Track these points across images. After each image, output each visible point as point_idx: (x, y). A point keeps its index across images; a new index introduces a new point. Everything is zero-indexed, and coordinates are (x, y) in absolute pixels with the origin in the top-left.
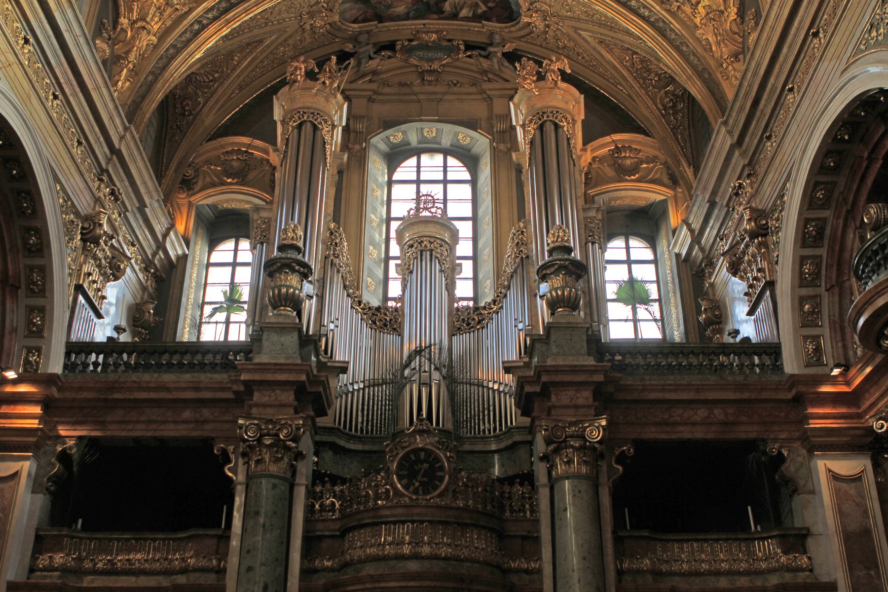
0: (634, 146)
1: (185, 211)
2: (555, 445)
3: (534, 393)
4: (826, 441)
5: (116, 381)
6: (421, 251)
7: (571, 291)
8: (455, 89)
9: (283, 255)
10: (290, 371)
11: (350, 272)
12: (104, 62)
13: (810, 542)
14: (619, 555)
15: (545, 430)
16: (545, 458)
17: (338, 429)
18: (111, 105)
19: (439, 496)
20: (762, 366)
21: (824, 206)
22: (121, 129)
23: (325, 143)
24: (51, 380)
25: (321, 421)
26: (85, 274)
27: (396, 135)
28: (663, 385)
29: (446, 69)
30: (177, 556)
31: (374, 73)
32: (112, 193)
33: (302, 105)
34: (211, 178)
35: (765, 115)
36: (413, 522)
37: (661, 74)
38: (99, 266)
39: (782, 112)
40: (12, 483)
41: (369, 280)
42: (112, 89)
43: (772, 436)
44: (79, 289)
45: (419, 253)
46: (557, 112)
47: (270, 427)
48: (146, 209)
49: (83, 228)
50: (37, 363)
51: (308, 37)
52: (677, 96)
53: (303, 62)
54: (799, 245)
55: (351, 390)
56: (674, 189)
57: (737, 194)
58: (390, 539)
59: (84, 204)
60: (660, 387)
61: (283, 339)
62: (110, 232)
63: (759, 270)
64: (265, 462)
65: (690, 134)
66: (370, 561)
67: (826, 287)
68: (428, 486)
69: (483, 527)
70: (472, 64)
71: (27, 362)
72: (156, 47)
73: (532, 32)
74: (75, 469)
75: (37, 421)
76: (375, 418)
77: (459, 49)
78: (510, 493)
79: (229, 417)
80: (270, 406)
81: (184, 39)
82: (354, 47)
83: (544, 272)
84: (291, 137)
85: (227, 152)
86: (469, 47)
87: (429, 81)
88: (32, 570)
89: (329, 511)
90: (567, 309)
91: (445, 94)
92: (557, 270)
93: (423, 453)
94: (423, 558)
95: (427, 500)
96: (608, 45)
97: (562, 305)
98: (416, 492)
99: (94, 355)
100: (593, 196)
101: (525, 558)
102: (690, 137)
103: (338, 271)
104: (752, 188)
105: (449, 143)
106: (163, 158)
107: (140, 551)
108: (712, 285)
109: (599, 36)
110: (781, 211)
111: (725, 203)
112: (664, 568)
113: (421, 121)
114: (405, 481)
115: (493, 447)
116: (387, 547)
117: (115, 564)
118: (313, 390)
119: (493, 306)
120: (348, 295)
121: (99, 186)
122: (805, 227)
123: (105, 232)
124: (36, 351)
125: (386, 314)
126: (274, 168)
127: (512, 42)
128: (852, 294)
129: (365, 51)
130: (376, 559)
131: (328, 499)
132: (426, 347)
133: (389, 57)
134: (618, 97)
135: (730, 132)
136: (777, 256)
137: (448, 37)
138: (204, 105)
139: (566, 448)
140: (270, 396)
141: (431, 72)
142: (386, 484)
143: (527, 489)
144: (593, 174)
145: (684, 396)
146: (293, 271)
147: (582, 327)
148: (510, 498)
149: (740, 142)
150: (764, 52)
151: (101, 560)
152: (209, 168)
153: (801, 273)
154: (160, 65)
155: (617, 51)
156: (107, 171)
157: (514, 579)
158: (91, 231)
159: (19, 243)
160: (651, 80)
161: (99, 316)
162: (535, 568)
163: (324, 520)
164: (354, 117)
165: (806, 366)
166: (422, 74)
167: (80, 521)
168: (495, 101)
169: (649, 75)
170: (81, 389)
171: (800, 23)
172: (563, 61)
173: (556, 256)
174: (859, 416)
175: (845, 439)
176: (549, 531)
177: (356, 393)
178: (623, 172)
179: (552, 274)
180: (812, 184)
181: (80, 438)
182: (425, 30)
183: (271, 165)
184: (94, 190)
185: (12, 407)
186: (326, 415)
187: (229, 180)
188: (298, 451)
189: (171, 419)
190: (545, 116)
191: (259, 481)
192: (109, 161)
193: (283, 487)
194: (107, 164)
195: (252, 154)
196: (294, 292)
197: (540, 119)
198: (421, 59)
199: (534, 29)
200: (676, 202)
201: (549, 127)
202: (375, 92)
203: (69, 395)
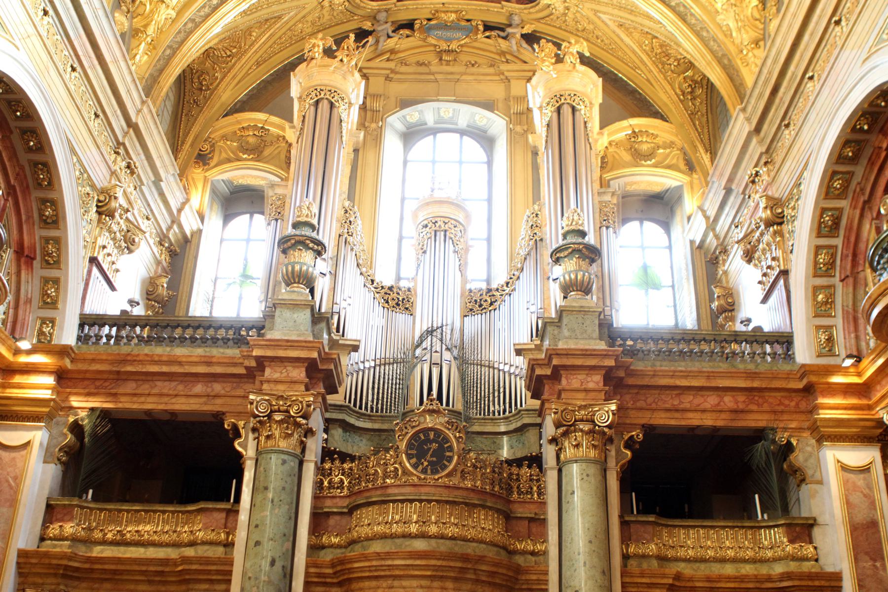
0: (651, 131)
1: (200, 186)
2: (564, 428)
3: (546, 376)
4: (835, 432)
5: (129, 355)
6: (436, 231)
7: (584, 275)
8: (474, 70)
9: (298, 232)
10: (303, 348)
11: (363, 250)
12: (123, 35)
13: (816, 532)
14: (626, 539)
15: (555, 413)
16: (553, 441)
17: (348, 407)
18: (129, 79)
19: (449, 475)
20: (774, 355)
21: (839, 197)
22: (138, 102)
23: (341, 121)
24: (63, 351)
25: (332, 399)
26: (100, 247)
27: (412, 114)
28: (675, 371)
29: (465, 49)
30: (186, 528)
31: (392, 51)
32: (128, 167)
33: (319, 82)
34: (227, 153)
35: (784, 103)
36: (420, 501)
37: (680, 59)
38: (114, 239)
39: (801, 100)
40: (24, 453)
42: (130, 63)
43: (781, 425)
44: (93, 260)
45: (433, 233)
46: (575, 95)
47: (281, 403)
48: (162, 183)
49: (99, 201)
50: (51, 334)
51: (326, 14)
52: (696, 82)
53: (321, 39)
54: (814, 234)
55: (362, 368)
56: (690, 175)
57: (753, 182)
58: (397, 517)
59: (101, 177)
60: (671, 374)
61: (295, 316)
62: (125, 205)
63: (773, 259)
64: (275, 438)
65: (708, 120)
66: (378, 539)
67: (840, 276)
68: (437, 465)
69: (490, 508)
70: (491, 45)
71: (41, 333)
72: (174, 21)
73: (552, 14)
74: (86, 440)
75: (50, 392)
76: (385, 396)
77: (478, 30)
78: (518, 475)
79: (240, 392)
80: (281, 382)
81: (202, 13)
82: (373, 25)
83: (558, 255)
84: (307, 114)
85: (243, 128)
86: (488, 27)
87: (447, 61)
88: (42, 539)
89: (338, 488)
90: (579, 293)
91: (462, 74)
92: (571, 253)
93: (433, 433)
94: (430, 537)
95: (435, 479)
96: (627, 29)
97: (575, 289)
98: (424, 471)
99: (107, 328)
100: (609, 181)
101: (532, 540)
102: (708, 123)
103: (352, 249)
104: (769, 176)
106: (179, 132)
107: (149, 523)
108: (725, 273)
109: (619, 19)
110: (797, 200)
111: (741, 190)
112: (670, 553)
113: (438, 100)
114: (414, 460)
115: (503, 429)
116: (395, 525)
117: (125, 535)
118: (325, 367)
119: (505, 288)
120: (361, 274)
121: (116, 158)
122: (821, 217)
123: (120, 206)
124: (50, 322)
125: (398, 294)
126: (290, 145)
127: (532, 24)
128: (866, 285)
129: (383, 30)
130: (384, 537)
131: (336, 476)
132: (438, 328)
133: (408, 36)
134: (637, 82)
135: (748, 120)
136: (792, 245)
137: (466, 17)
138: (222, 80)
139: (575, 431)
140: (281, 373)
141: (449, 52)
142: (395, 463)
143: (535, 471)
144: (610, 159)
146: (307, 248)
147: (594, 311)
148: (518, 480)
149: (758, 129)
150: (784, 39)
151: (111, 531)
152: (225, 143)
153: (816, 263)
154: (178, 39)
155: (636, 35)
156: (124, 144)
157: (520, 560)
158: (106, 204)
159: (36, 215)
160: (670, 65)
161: (112, 288)
162: (541, 550)
163: (333, 497)
164: (371, 95)
165: (818, 356)
166: (440, 54)
167: (91, 491)
168: (513, 82)
169: (668, 60)
170: (93, 360)
171: (823, 10)
172: (582, 43)
173: (570, 239)
174: (870, 408)
175: (855, 430)
176: (556, 514)
177: (367, 371)
178: (639, 157)
179: (565, 257)
180: (829, 173)
181: (92, 410)
182: (444, 9)
183: (287, 142)
184: (110, 163)
185: (25, 377)
186: (337, 392)
187: (245, 156)
188: (308, 428)
189: (182, 393)
190: (563, 98)
191: (269, 456)
192: (126, 134)
193: (292, 464)
194: (124, 137)
195: (268, 130)
196: (307, 270)
197: (558, 102)
198: (439, 38)
199: (554, 11)
200: (692, 188)
201: (567, 111)
202: (393, 71)
203: (81, 366)
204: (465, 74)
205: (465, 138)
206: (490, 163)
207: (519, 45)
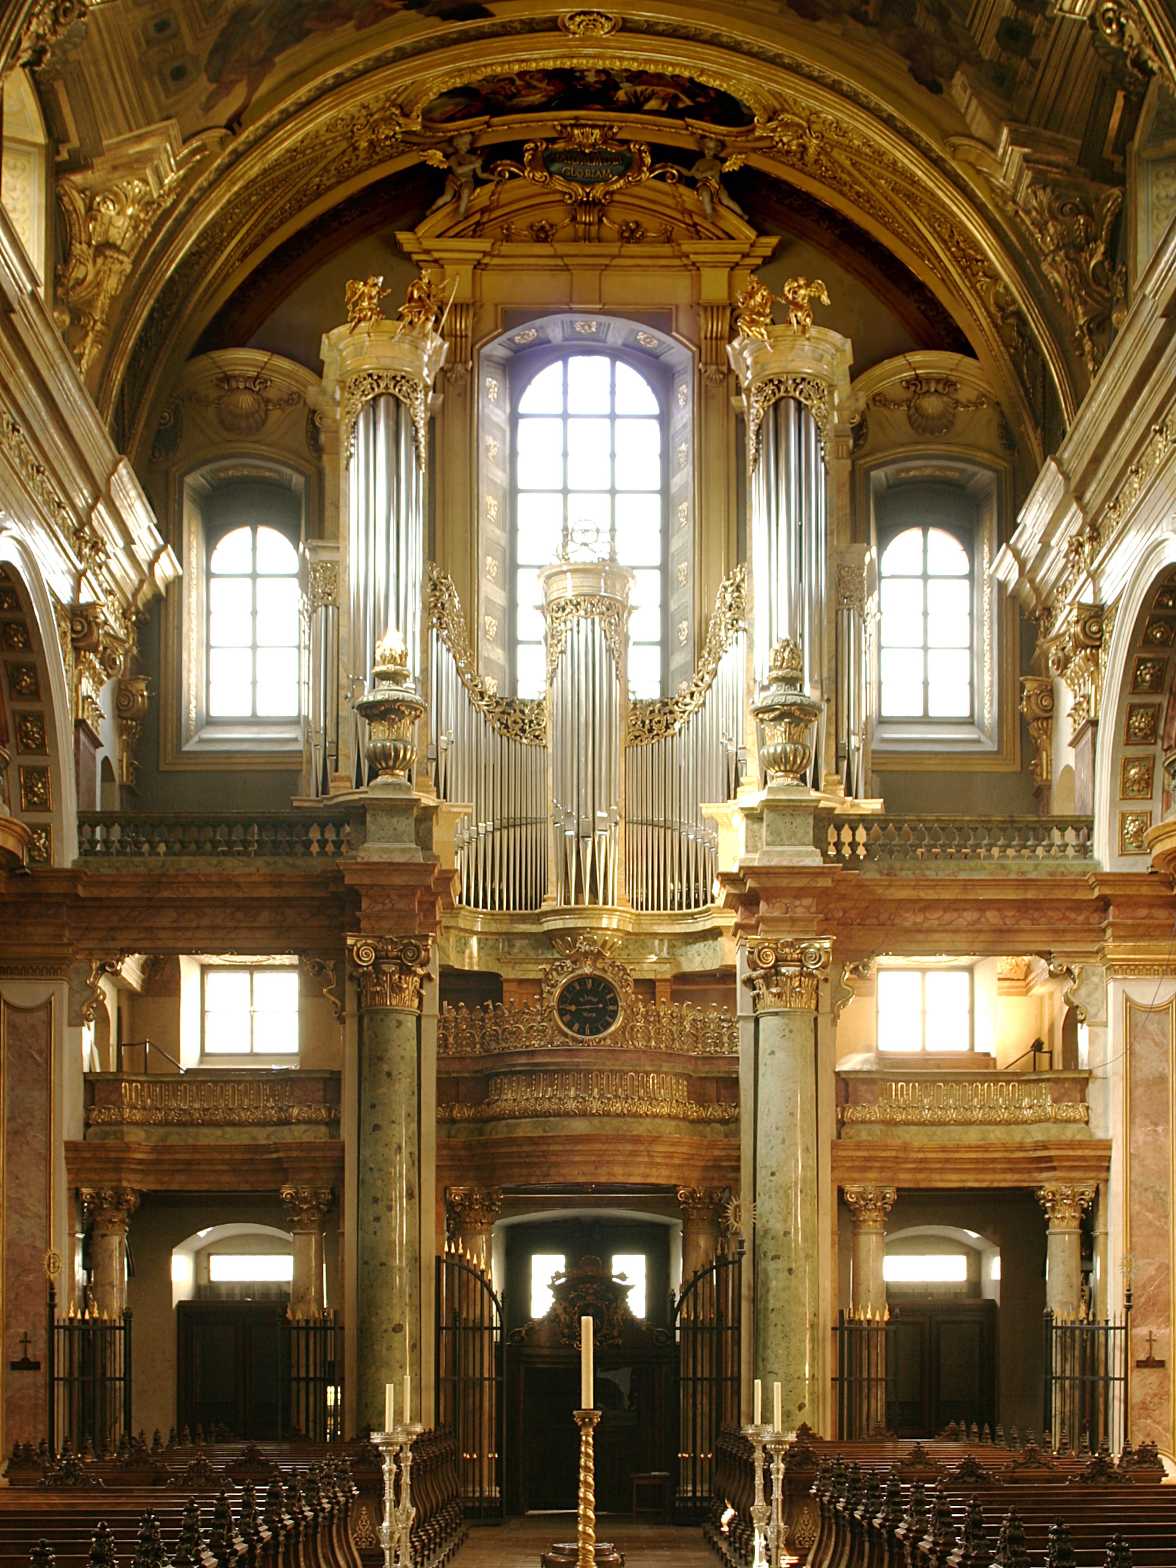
27: (525, 334)
29: (617, 197)
41: (488, 619)
70: (665, 194)
77: (643, 163)
91: (613, 257)
105: (620, 342)
113: (571, 311)
125: (522, 712)
133: (513, 176)
137: (620, 136)
145: (946, 895)
168: (705, 272)
170: (114, 883)
198: (568, 178)
202: (485, 254)
203: (97, 892)
204: (619, 256)
205: (619, 364)
206: (664, 419)
207: (716, 200)
